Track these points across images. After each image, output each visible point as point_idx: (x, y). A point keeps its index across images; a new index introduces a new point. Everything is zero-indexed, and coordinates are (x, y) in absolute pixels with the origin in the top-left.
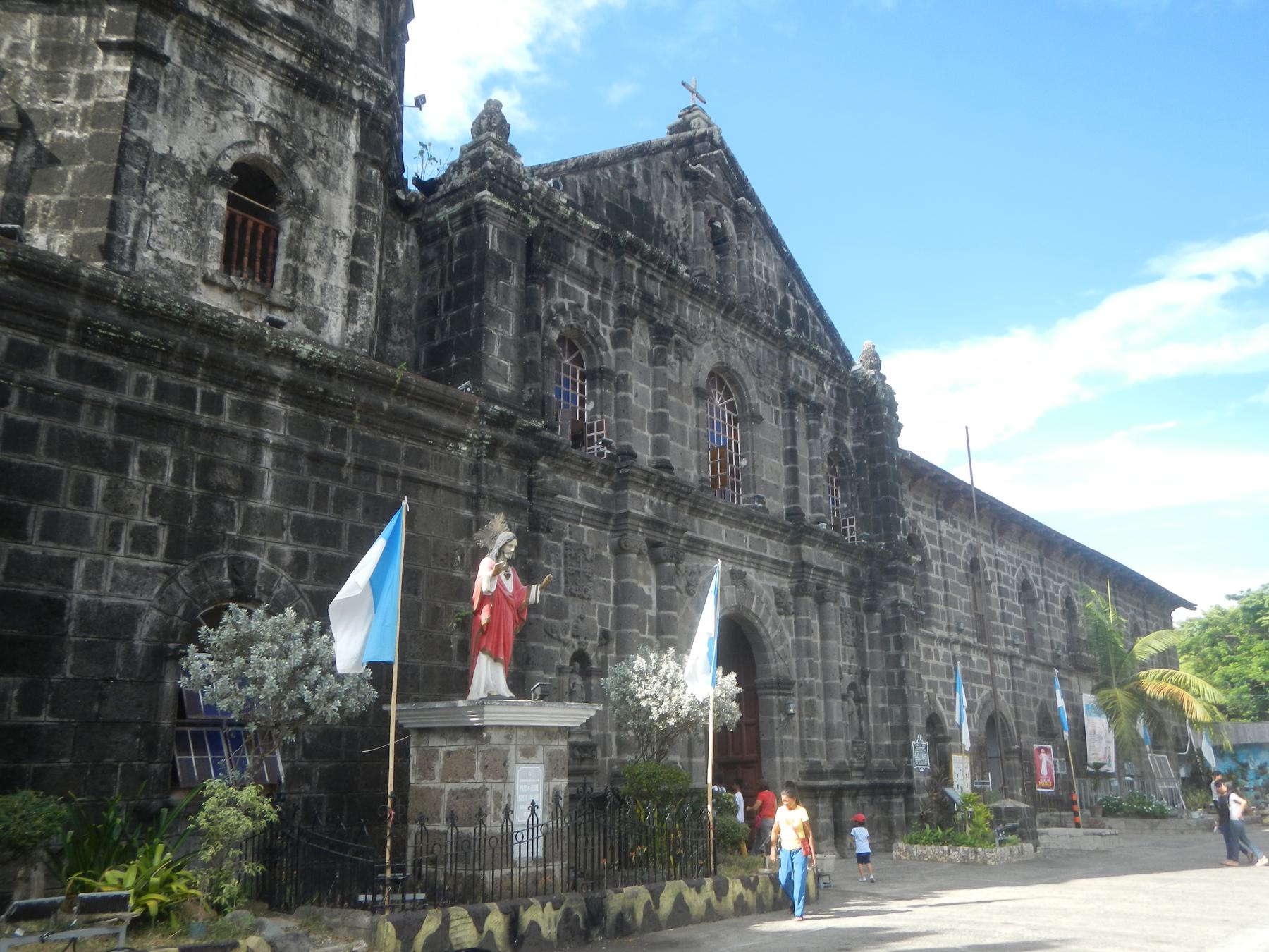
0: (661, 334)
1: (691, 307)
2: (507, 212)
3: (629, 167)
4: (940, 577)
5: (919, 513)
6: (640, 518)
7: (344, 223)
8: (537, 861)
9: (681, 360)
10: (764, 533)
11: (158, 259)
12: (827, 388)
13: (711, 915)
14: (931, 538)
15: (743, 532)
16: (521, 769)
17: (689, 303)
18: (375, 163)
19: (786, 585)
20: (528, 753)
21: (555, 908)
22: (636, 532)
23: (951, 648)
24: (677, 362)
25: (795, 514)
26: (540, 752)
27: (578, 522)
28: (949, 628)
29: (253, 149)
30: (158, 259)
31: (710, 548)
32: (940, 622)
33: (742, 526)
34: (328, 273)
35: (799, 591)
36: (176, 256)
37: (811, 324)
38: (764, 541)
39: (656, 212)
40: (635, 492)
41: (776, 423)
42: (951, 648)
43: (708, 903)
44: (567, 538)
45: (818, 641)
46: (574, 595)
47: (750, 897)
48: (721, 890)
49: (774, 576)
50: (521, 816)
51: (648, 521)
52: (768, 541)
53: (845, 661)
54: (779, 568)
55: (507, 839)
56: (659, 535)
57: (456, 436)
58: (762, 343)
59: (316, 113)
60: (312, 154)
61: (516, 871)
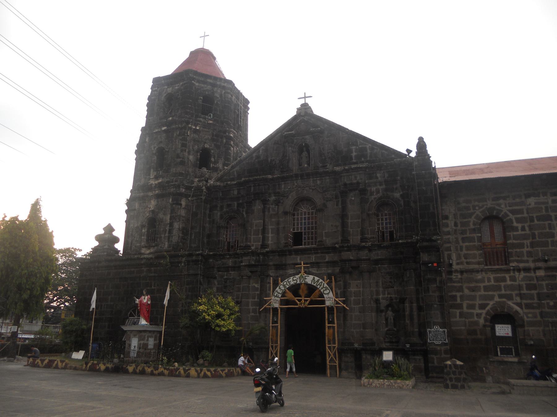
0: (265, 202)
1: (284, 184)
2: (196, 199)
3: (259, 151)
4: (528, 232)
5: (501, 201)
6: (245, 266)
7: (168, 221)
8: (136, 358)
9: (277, 205)
10: (322, 253)
11: (135, 246)
12: (378, 175)
13: (152, 374)
14: (513, 212)
15: (310, 256)
16: (133, 339)
17: (283, 183)
18: (174, 204)
19: (337, 270)
20: (135, 336)
21: (113, 365)
22: (246, 270)
23: (535, 273)
24: (277, 207)
25: (345, 240)
26: (137, 336)
27: (229, 271)
28: (534, 261)
29: (149, 217)
30: (135, 246)
31: (288, 266)
32: (525, 258)
33: (309, 254)
34: (165, 235)
35: (342, 272)
36: (138, 245)
37: (369, 151)
38: (325, 256)
39: (269, 160)
40: (245, 258)
41: (337, 205)
42: (535, 273)
43: (152, 371)
44: (225, 277)
45: (361, 289)
46: (225, 292)
47: (166, 372)
48: (157, 369)
49: (329, 268)
50: (132, 348)
51: (250, 266)
52: (326, 255)
53: (384, 294)
54: (333, 263)
55: (129, 353)
56: (255, 269)
57: (181, 262)
58: (327, 177)
59: (163, 200)
60: (162, 210)
61: (130, 359)
